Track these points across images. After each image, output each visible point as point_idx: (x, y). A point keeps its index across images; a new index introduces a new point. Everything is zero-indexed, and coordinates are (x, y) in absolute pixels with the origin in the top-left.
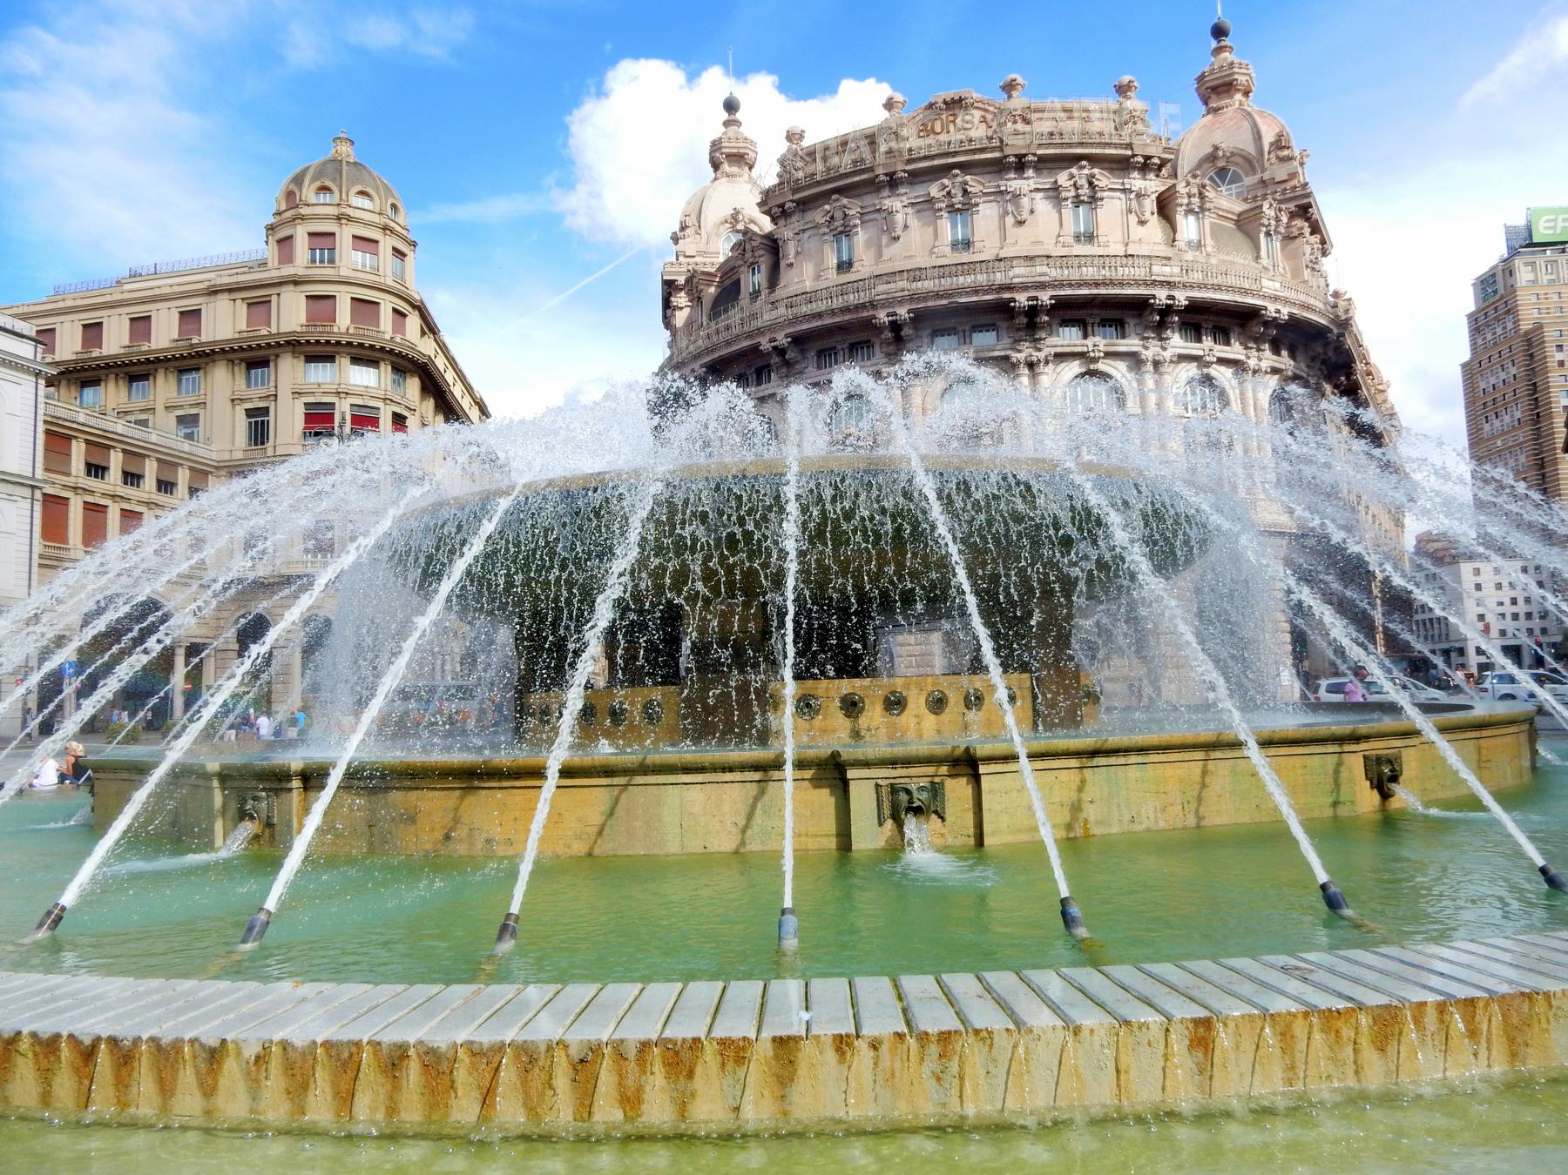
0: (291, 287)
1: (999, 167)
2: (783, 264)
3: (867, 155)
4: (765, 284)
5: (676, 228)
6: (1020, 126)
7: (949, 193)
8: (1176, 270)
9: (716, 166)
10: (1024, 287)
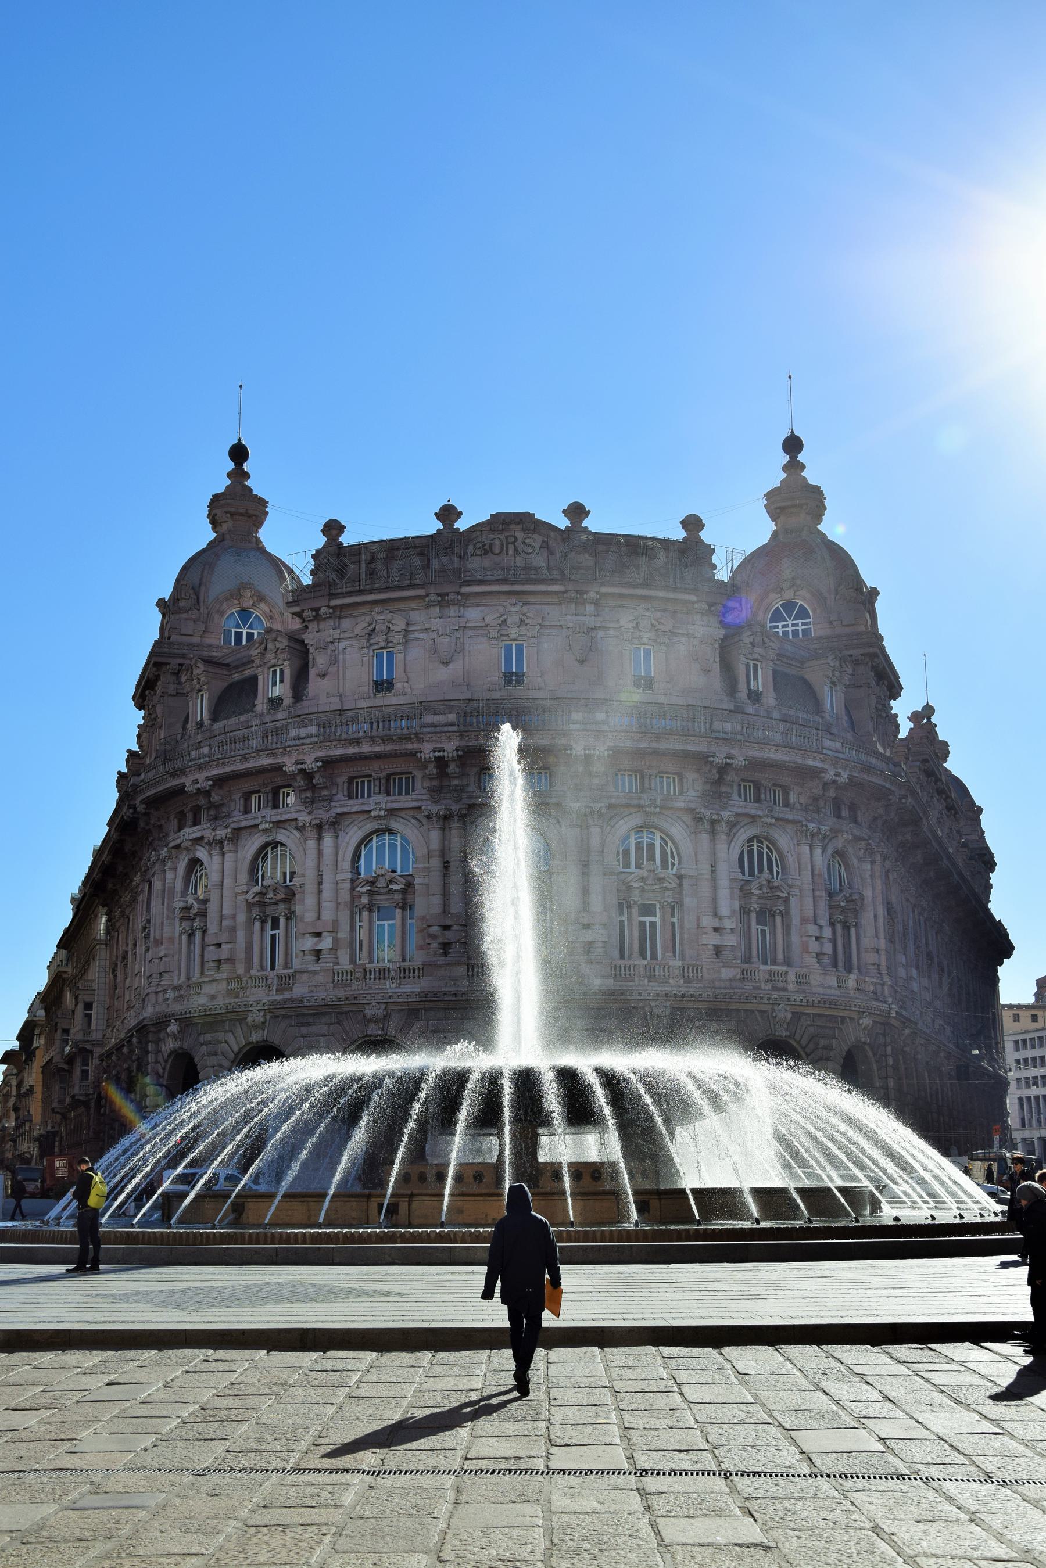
2: (312, 672)
8: (738, 727)
9: (214, 522)
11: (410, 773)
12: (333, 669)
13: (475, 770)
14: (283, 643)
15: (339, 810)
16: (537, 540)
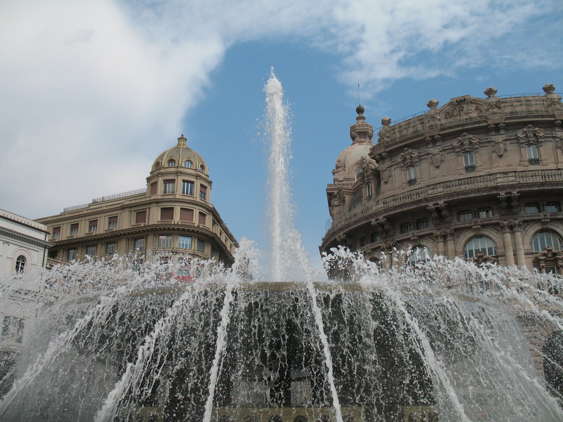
0: (155, 205)
1: (487, 130)
2: (382, 182)
3: (419, 127)
4: (374, 192)
5: (334, 168)
6: (495, 110)
7: (462, 144)
9: (353, 138)
10: (503, 188)
11: (426, 218)
12: (390, 179)
13: (455, 212)
14: (370, 172)
15: (397, 239)
16: (473, 107)
